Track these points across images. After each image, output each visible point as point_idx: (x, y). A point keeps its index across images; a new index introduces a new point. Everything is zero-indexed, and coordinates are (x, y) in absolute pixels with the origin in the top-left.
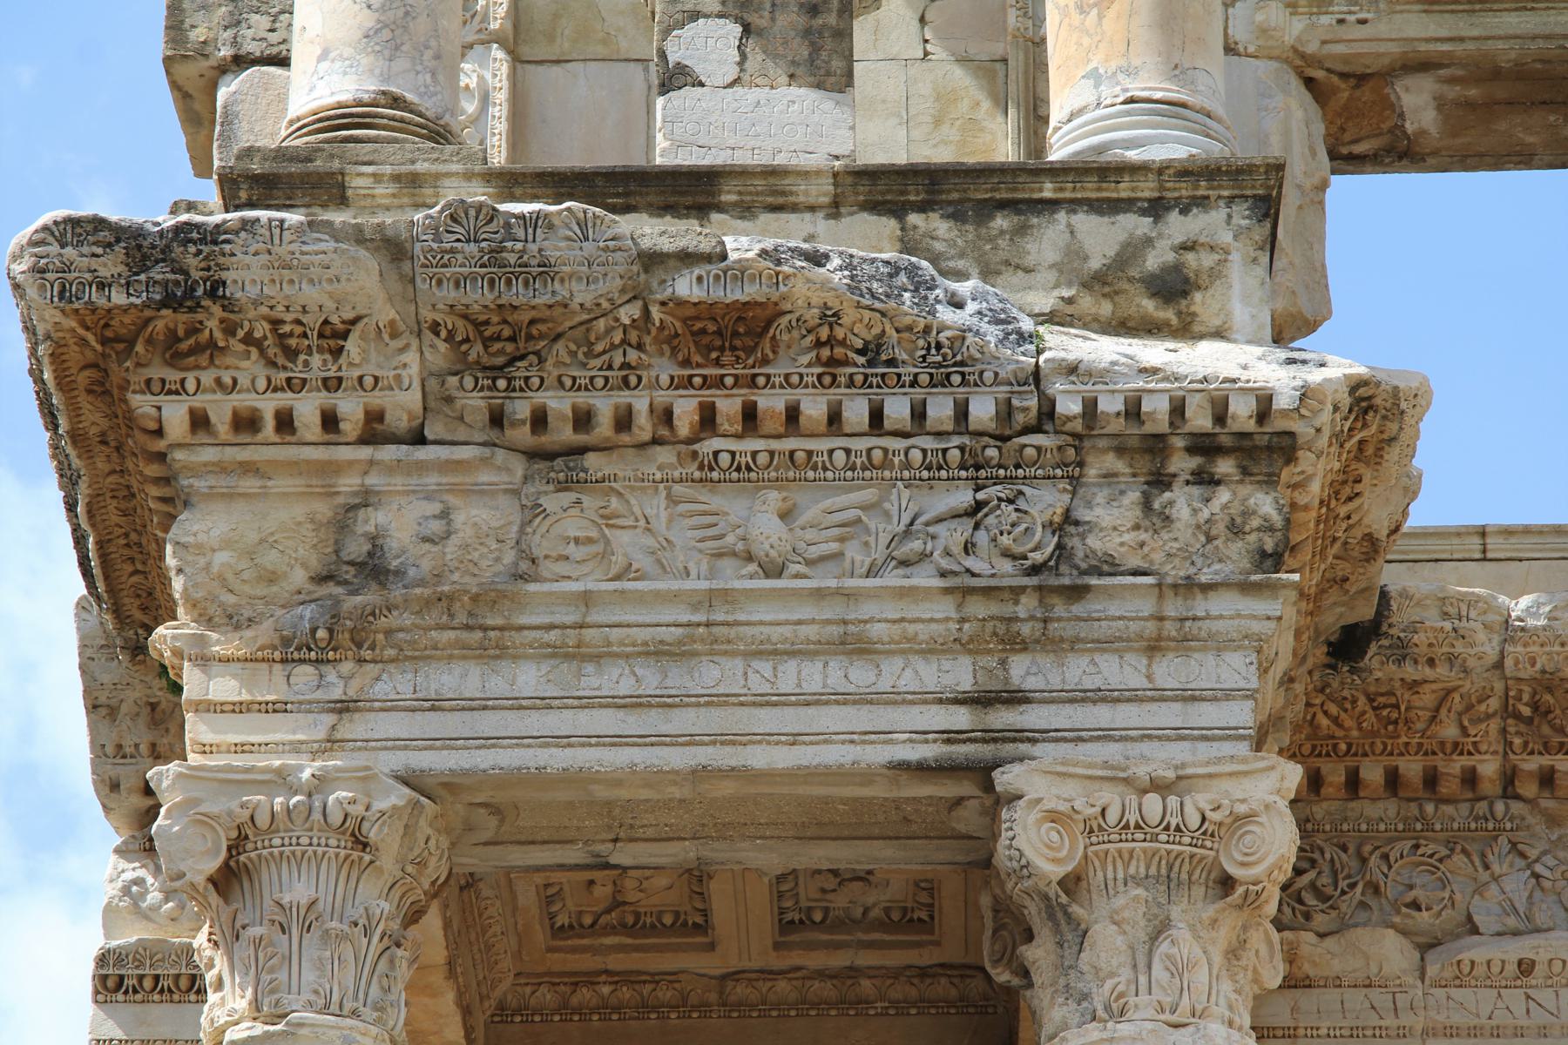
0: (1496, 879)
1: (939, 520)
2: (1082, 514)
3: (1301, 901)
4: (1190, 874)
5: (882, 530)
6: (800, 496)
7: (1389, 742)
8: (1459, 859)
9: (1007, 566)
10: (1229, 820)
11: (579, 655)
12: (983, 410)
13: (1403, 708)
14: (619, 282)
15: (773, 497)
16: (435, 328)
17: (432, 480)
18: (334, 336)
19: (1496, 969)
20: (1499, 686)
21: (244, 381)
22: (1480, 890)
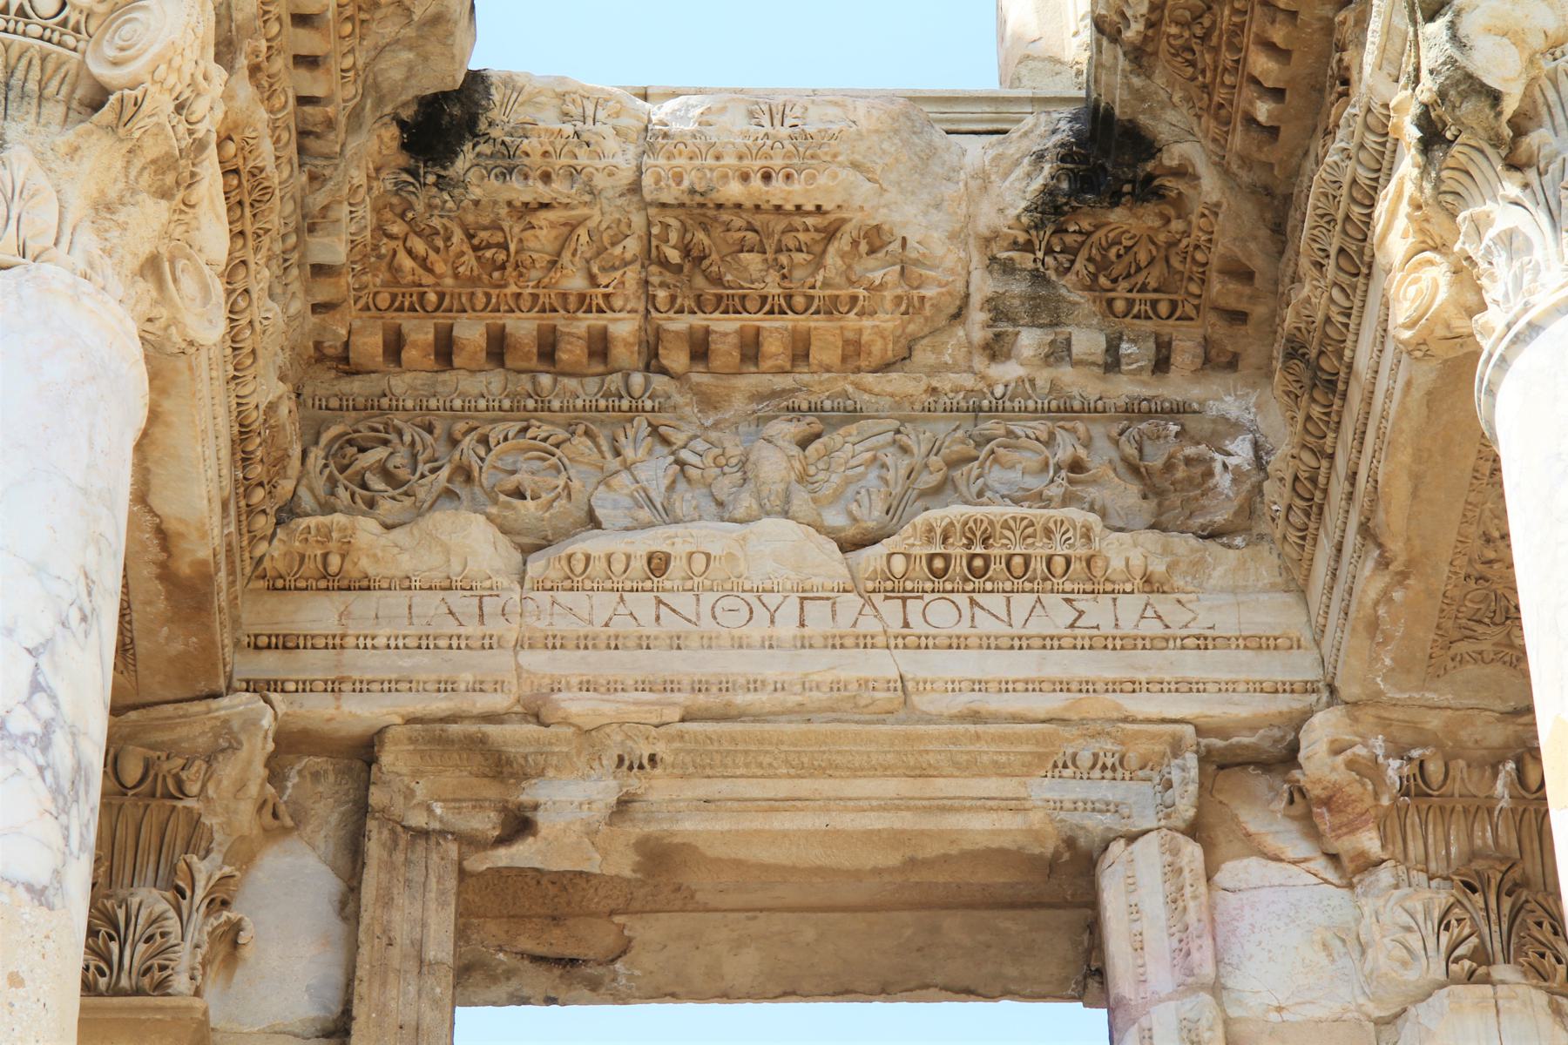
0: (628, 467)
3: (364, 486)
4: (42, 86)
7: (494, 292)
8: (581, 443)
13: (512, 247)
19: (618, 567)
20: (638, 220)
22: (605, 481)
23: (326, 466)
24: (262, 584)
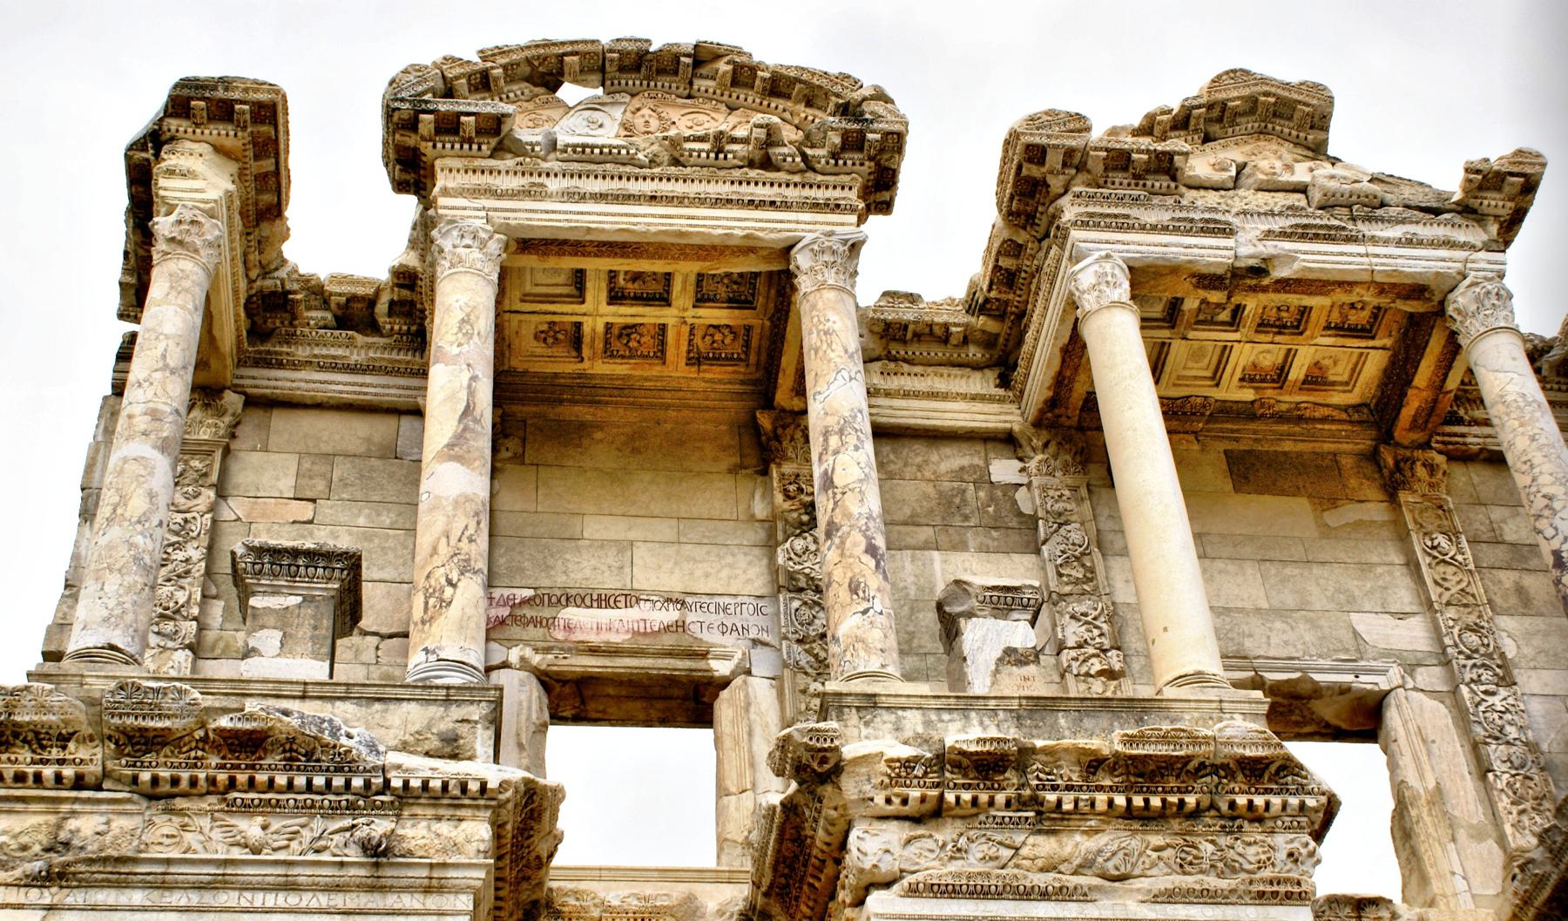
2: (400, 832)
5: (307, 835)
6: (270, 819)
11: (164, 886)
12: (357, 782)
15: (260, 820)
17: (104, 807)
18: (64, 740)
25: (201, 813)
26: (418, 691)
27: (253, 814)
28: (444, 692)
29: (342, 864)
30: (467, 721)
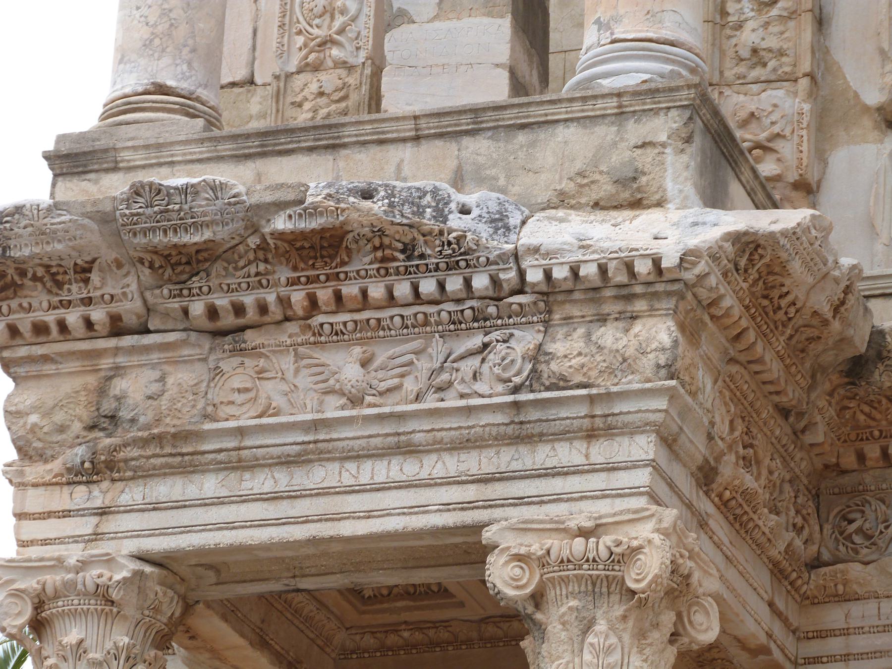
1: (462, 358)
2: (551, 347)
4: (608, 587)
5: (424, 365)
9: (500, 388)
10: (628, 551)
11: (240, 465)
12: (481, 282)
14: (241, 223)
15: (357, 350)
16: (141, 261)
17: (155, 356)
18: (84, 271)
21: (35, 304)
23: (834, 532)
24: (807, 602)
25: (281, 349)
26: (577, 106)
27: (352, 343)
28: (614, 102)
29: (469, 410)
30: (651, 144)
